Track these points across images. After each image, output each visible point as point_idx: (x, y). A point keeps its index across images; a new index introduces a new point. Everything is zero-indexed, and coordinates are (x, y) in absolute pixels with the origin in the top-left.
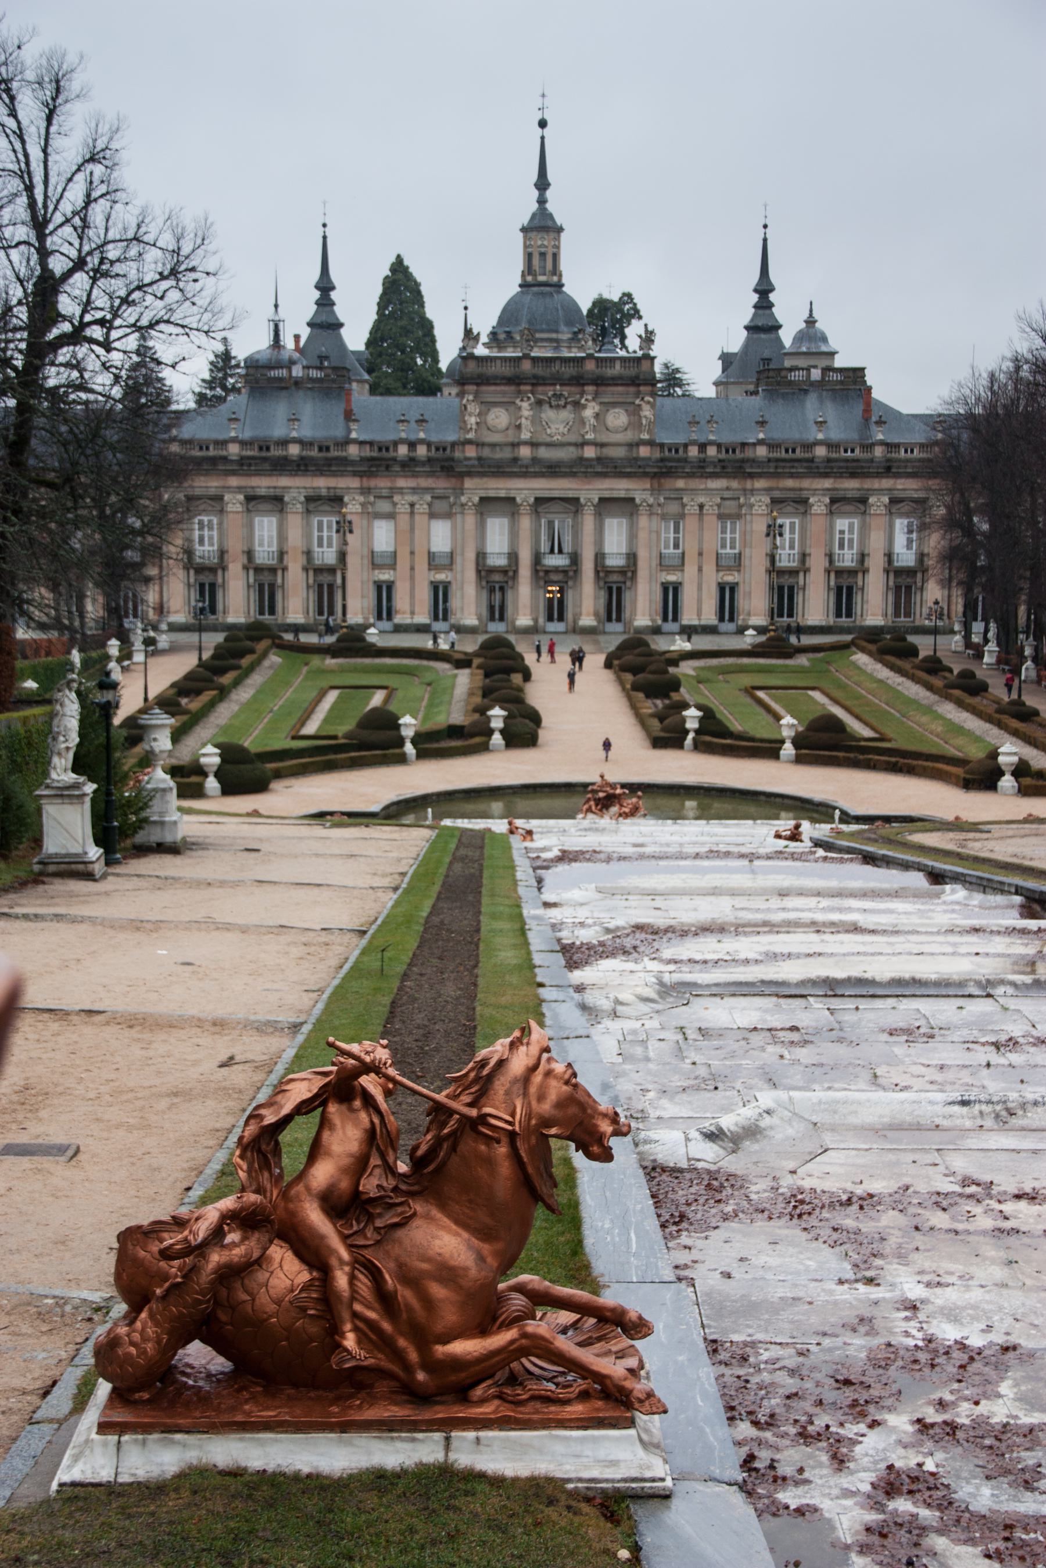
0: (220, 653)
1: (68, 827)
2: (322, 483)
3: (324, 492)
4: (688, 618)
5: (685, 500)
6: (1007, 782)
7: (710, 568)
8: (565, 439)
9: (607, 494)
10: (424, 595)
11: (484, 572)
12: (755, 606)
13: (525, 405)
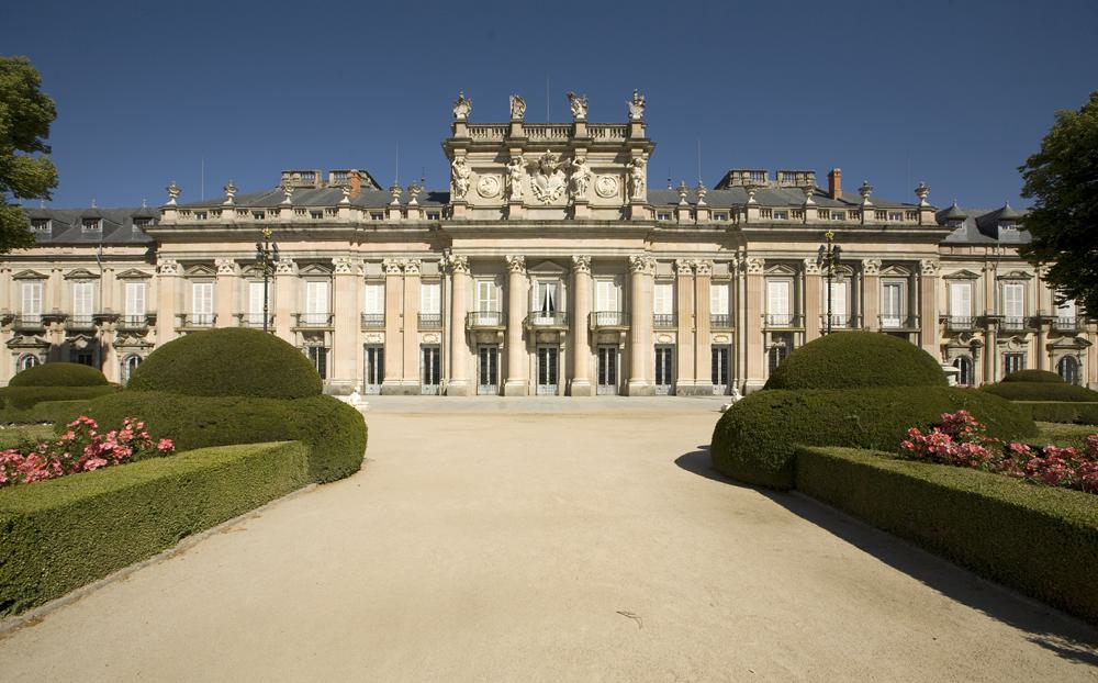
2: (310, 248)
3: (313, 255)
4: (684, 380)
5: (678, 262)
7: (703, 329)
8: (553, 203)
9: (599, 254)
10: (417, 358)
13: (516, 167)
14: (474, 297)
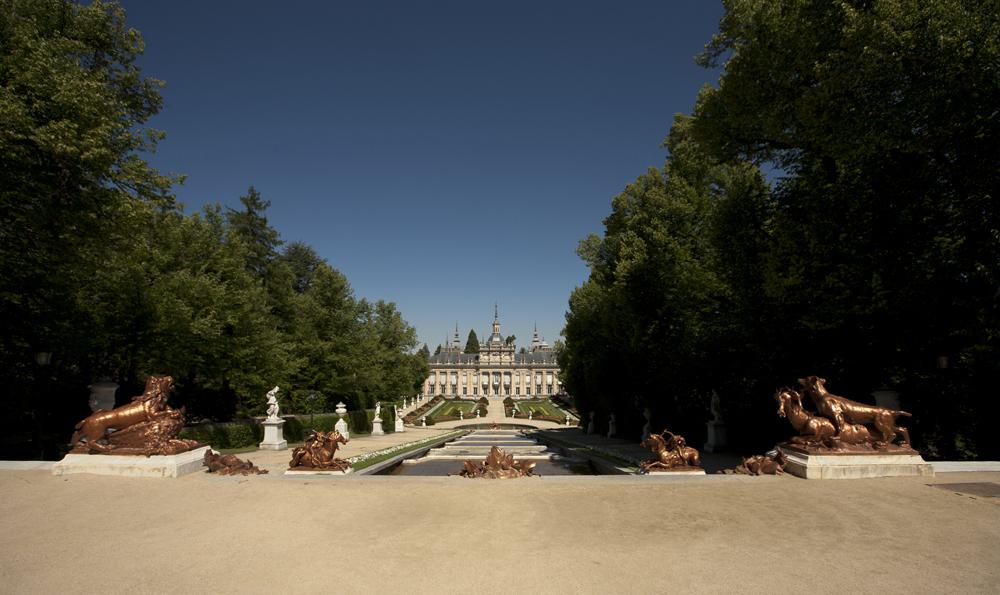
0: (433, 400)
1: (377, 428)
2: (454, 370)
6: (568, 423)
10: (473, 390)
11: (483, 386)
12: (534, 392)
14: (485, 380)
